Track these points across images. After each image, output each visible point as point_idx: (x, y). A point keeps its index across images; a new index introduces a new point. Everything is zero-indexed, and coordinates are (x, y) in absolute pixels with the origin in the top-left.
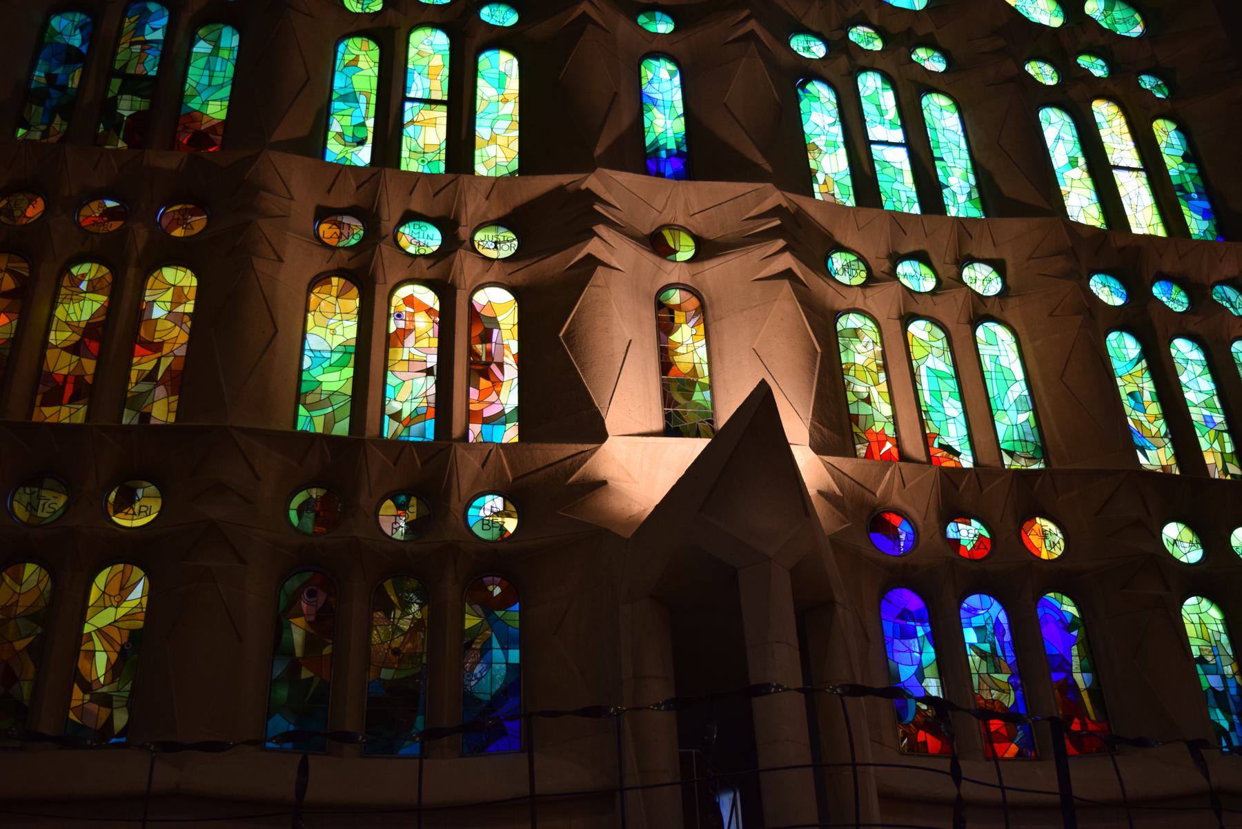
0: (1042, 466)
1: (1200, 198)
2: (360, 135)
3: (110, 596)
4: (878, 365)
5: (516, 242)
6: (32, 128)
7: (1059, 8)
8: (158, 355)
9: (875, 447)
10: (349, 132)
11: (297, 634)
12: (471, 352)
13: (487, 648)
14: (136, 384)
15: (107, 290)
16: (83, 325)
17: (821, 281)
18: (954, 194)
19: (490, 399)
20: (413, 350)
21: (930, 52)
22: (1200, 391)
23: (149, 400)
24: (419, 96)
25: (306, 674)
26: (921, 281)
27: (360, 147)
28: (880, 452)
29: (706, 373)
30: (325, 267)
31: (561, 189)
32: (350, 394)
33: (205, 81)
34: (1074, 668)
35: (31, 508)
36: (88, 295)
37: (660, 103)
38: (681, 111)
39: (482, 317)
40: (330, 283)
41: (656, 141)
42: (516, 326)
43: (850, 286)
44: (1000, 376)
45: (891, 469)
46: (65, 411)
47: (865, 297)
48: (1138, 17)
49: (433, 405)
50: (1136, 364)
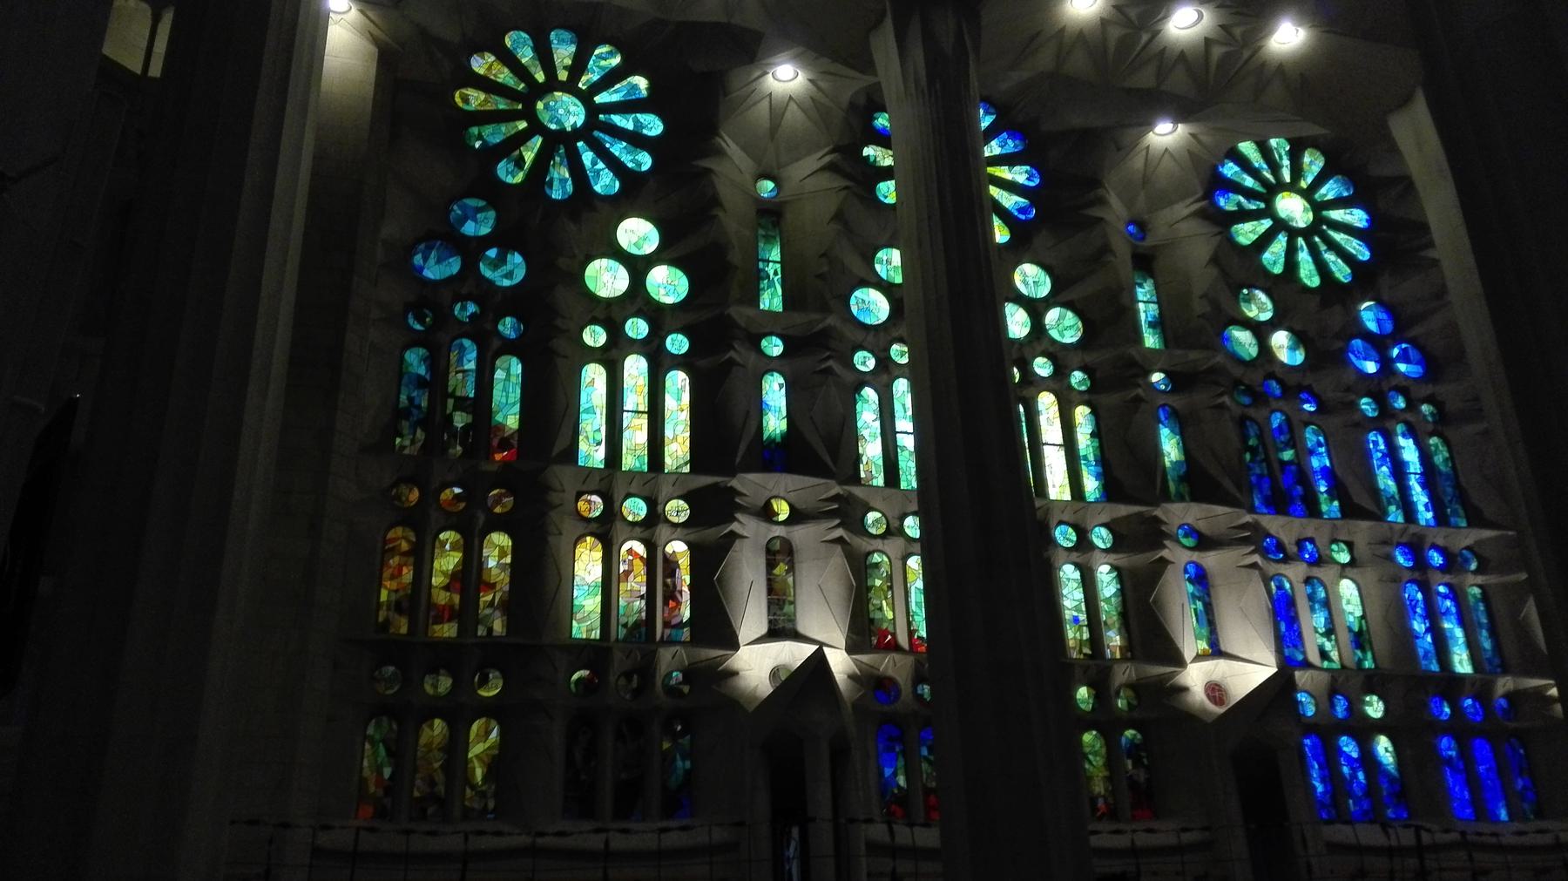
4: (888, 587)
5: (688, 511)
14: (484, 609)
15: (462, 549)
16: (450, 572)
25: (583, 777)
29: (792, 594)
31: (716, 485)
33: (504, 400)
35: (435, 686)
36: (451, 553)
37: (773, 408)
38: (784, 414)
41: (770, 436)
46: (446, 626)
47: (883, 544)
48: (1080, 324)
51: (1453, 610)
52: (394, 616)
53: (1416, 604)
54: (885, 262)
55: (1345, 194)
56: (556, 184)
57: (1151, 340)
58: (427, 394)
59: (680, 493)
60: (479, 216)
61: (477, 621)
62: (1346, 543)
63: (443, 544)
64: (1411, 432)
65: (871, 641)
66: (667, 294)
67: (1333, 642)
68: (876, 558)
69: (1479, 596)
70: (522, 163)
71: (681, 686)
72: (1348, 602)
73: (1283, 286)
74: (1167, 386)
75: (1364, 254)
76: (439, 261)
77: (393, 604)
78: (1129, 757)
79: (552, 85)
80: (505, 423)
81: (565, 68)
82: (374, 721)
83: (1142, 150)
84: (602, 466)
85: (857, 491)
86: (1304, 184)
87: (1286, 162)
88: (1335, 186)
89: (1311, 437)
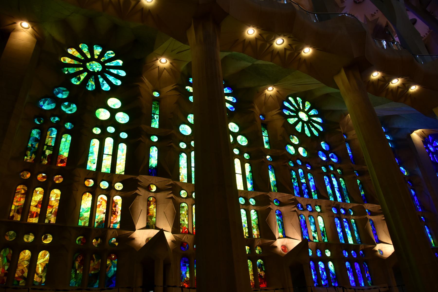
2: (94, 162)
4: (186, 214)
5: (122, 187)
8: (52, 208)
9: (184, 230)
11: (77, 264)
12: (112, 209)
13: (111, 267)
14: (48, 214)
15: (43, 194)
16: (38, 201)
17: (178, 198)
19: (115, 219)
20: (101, 209)
23: (50, 218)
25: (78, 272)
29: (155, 215)
31: (132, 178)
33: (64, 148)
35: (28, 239)
36: (39, 195)
39: (115, 203)
40: (86, 194)
41: (151, 165)
46: (34, 219)
47: (186, 200)
48: (247, 140)
51: (347, 226)
52: (16, 214)
53: (338, 224)
55: (316, 114)
56: (90, 86)
57: (266, 146)
58: (38, 144)
59: (120, 181)
60: (63, 92)
61: (45, 218)
62: (319, 206)
63: (36, 192)
64: (335, 177)
65: (180, 230)
66: (122, 121)
67: (316, 234)
68: (183, 204)
69: (354, 222)
71: (115, 243)
72: (320, 223)
73: (301, 136)
74: (271, 159)
75: (321, 129)
76: (48, 104)
77: (16, 210)
78: (259, 268)
79: (93, 59)
80: (63, 154)
81: (97, 55)
82: (3, 250)
83: (264, 95)
84: (95, 170)
85: (177, 183)
86: (306, 110)
87: (301, 104)
88: (313, 111)
89: (309, 176)
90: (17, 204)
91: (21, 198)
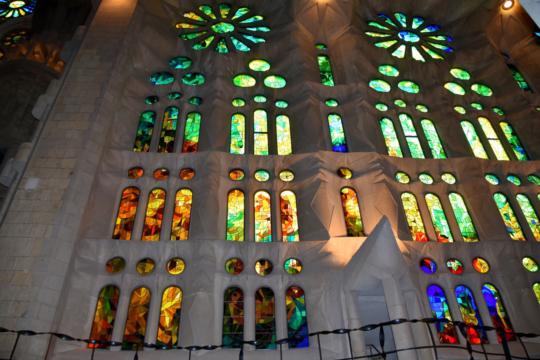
0: (477, 241)
1: (519, 147)
2: (241, 144)
3: (169, 298)
4: (417, 210)
5: (293, 176)
6: (138, 148)
7: (463, 89)
9: (419, 237)
10: (237, 144)
11: (231, 309)
12: (281, 212)
14: (175, 227)
16: (157, 209)
17: (395, 182)
18: (435, 151)
19: (289, 227)
20: (263, 212)
21: (422, 107)
22: (529, 212)
23: (179, 233)
24: (258, 131)
25: (235, 322)
26: (428, 180)
27: (241, 148)
28: (421, 238)
29: (359, 215)
30: (233, 187)
32: (243, 228)
33: (191, 130)
34: (497, 310)
36: (158, 200)
37: (335, 128)
38: (342, 131)
39: (284, 201)
42: (295, 203)
43: (404, 184)
44: (459, 211)
45: (426, 244)
46: (152, 237)
47: (410, 187)
48: (489, 90)
49: (271, 230)
50: (505, 204)
54: (384, 70)
60: (183, 63)
63: (154, 196)
70: (204, 45)
76: (163, 79)
77: (123, 225)
81: (225, 15)
90: (125, 216)
91: (130, 207)
